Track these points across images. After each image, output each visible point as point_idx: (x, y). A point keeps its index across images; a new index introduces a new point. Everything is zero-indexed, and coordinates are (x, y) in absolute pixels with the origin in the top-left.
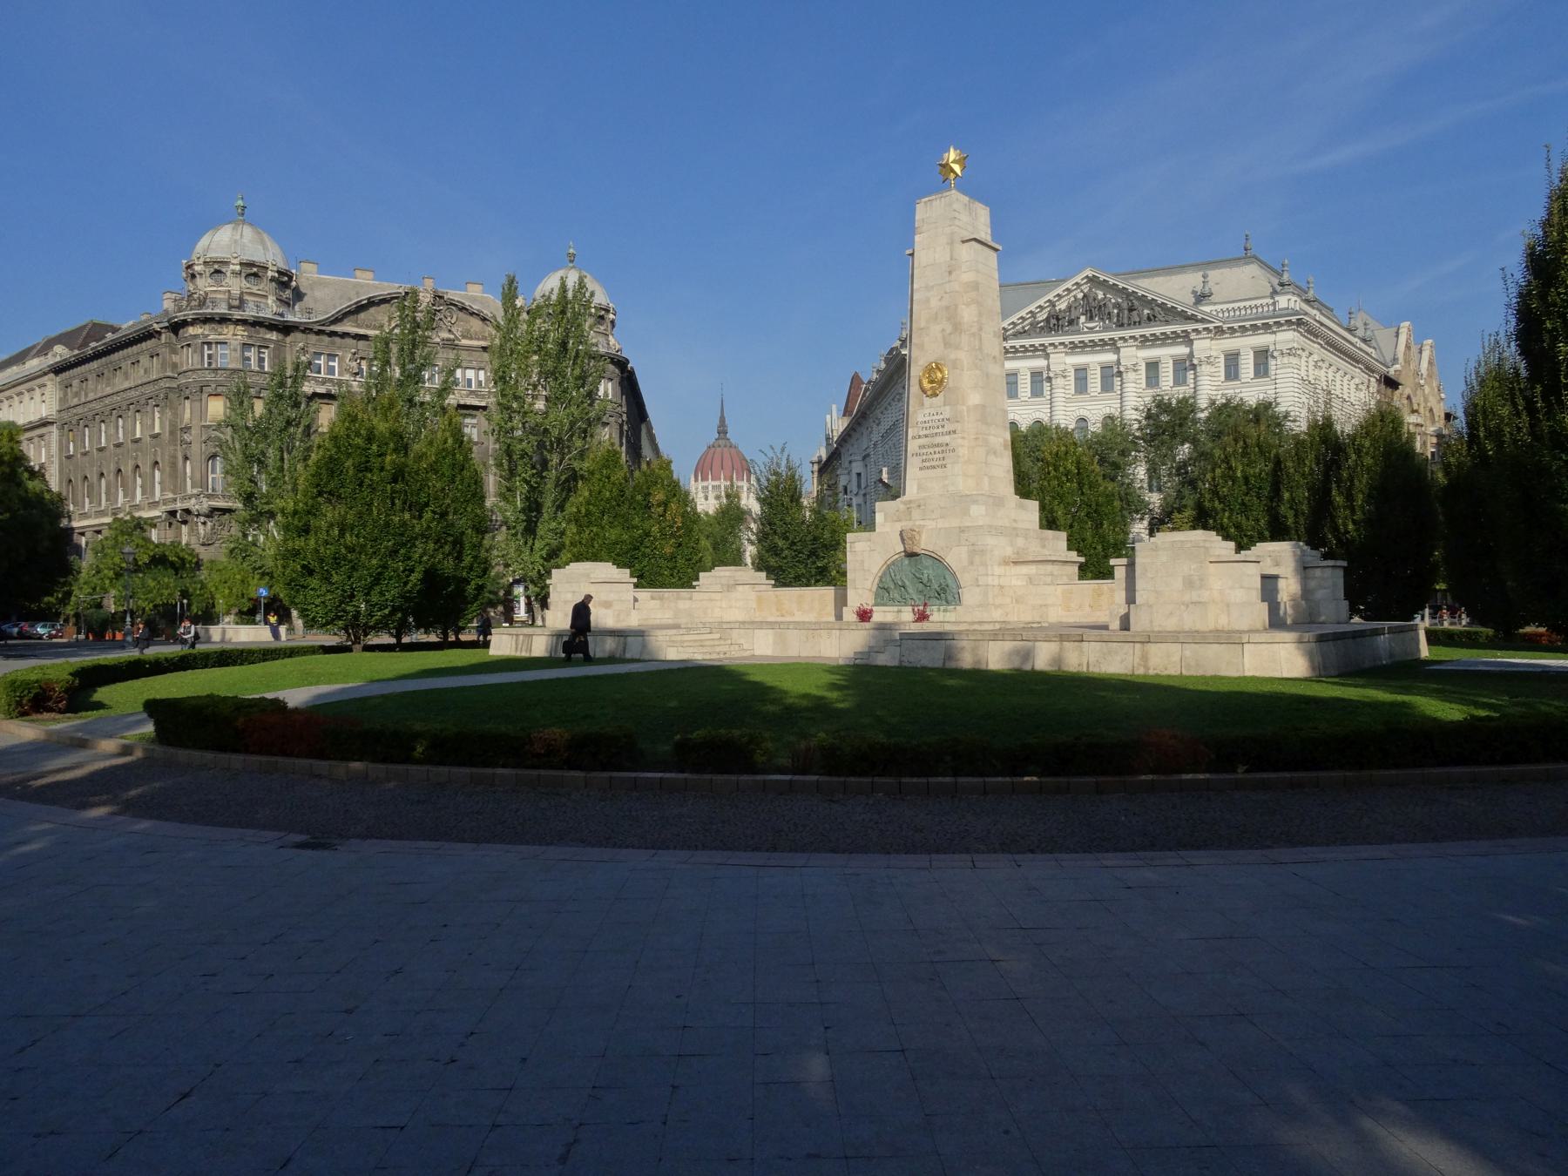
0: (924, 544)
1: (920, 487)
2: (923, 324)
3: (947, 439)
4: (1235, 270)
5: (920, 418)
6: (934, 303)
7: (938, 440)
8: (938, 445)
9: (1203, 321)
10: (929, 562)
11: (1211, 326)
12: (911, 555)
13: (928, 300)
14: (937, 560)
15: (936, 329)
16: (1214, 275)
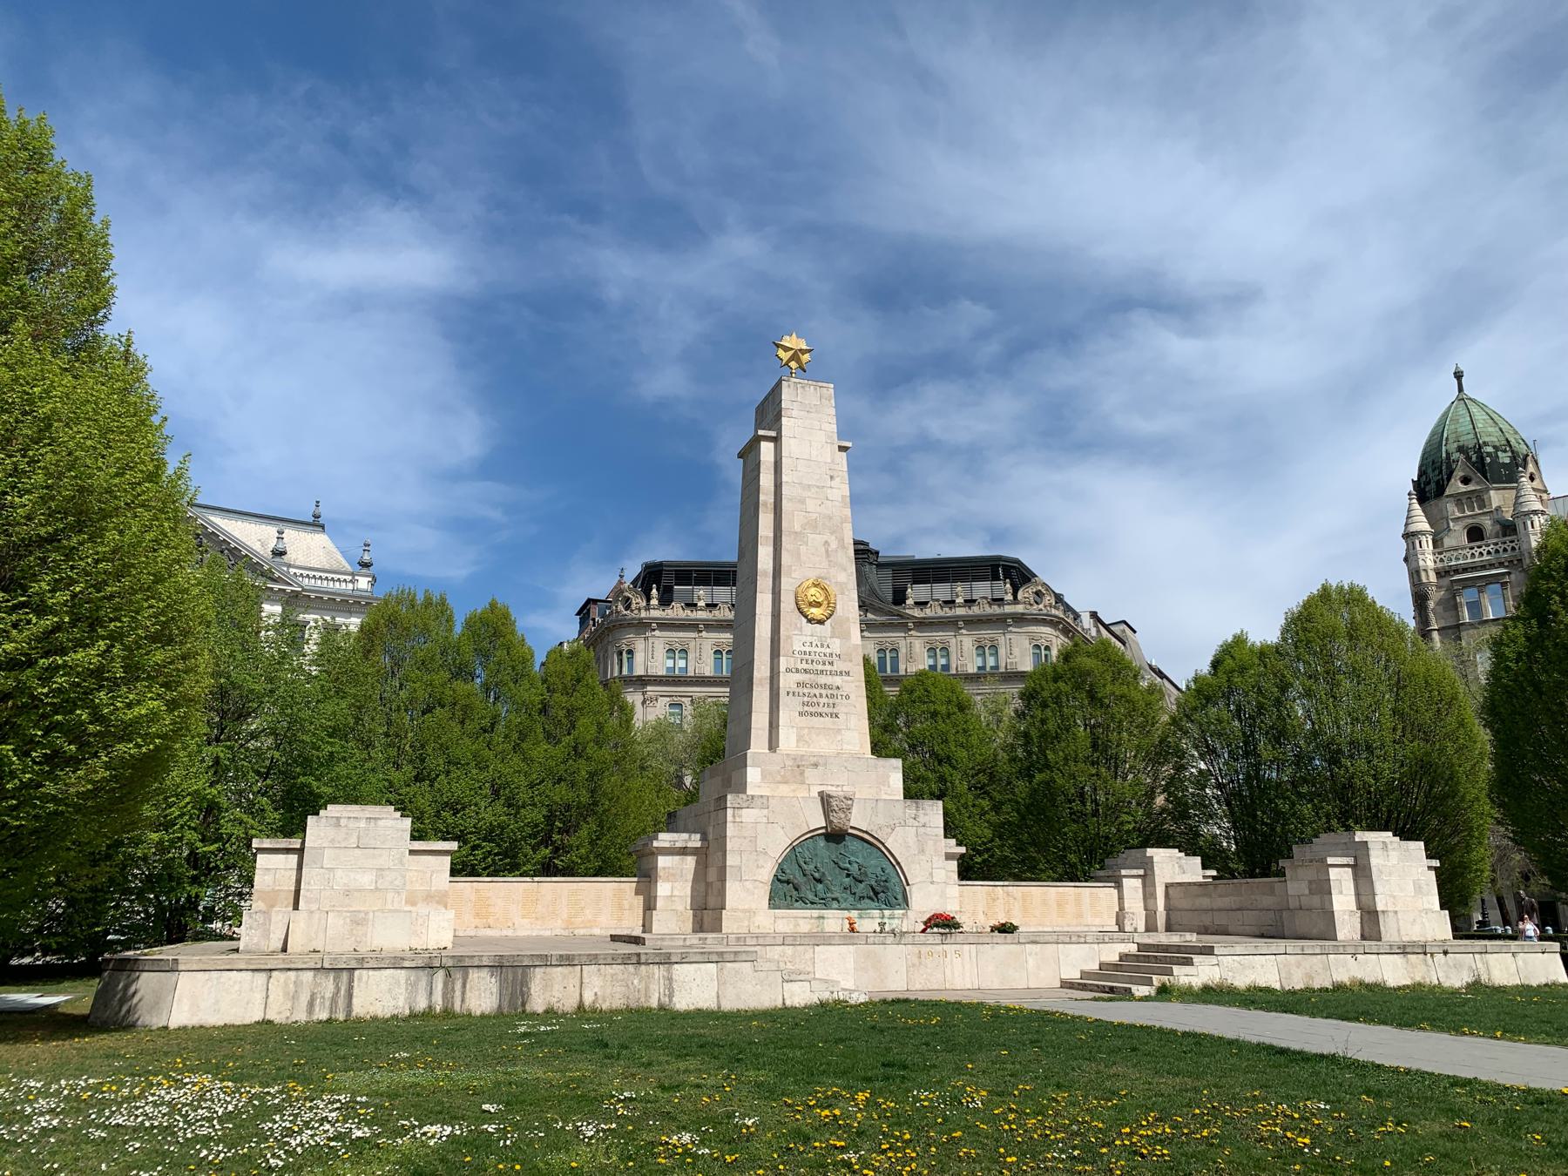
0: (858, 820)
1: (800, 739)
2: (797, 528)
3: (838, 680)
4: (302, 534)
5: (797, 647)
6: (811, 505)
7: (822, 680)
8: (825, 686)
9: (275, 580)
10: (854, 845)
11: (289, 589)
12: (835, 836)
13: (802, 501)
14: (871, 843)
15: (816, 540)
16: (290, 534)
